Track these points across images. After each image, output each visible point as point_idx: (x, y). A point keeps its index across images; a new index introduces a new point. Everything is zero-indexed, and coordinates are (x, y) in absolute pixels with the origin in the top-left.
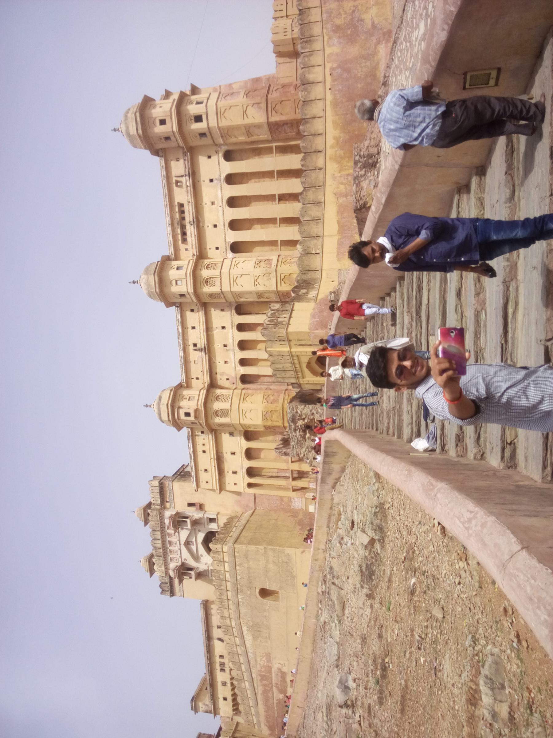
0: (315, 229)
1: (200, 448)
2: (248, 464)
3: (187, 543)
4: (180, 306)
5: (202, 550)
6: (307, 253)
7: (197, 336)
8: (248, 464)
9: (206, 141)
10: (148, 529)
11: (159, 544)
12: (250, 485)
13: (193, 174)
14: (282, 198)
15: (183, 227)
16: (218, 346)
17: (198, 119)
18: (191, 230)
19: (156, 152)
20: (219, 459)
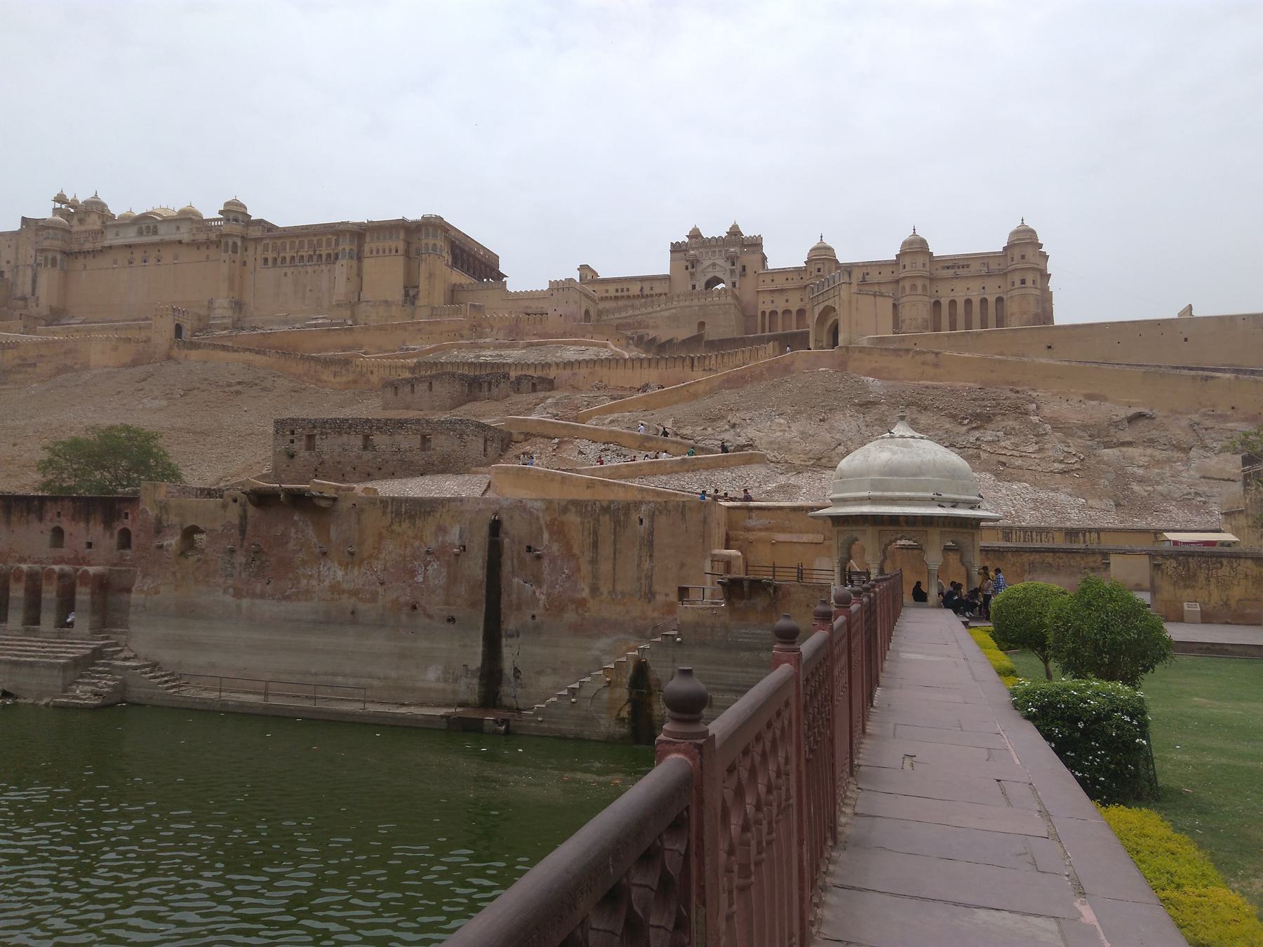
2: (780, 311)
3: (714, 265)
5: (709, 276)
8: (780, 311)
9: (1009, 284)
12: (763, 313)
13: (989, 275)
15: (953, 267)
17: (1023, 282)
18: (951, 272)
20: (782, 290)
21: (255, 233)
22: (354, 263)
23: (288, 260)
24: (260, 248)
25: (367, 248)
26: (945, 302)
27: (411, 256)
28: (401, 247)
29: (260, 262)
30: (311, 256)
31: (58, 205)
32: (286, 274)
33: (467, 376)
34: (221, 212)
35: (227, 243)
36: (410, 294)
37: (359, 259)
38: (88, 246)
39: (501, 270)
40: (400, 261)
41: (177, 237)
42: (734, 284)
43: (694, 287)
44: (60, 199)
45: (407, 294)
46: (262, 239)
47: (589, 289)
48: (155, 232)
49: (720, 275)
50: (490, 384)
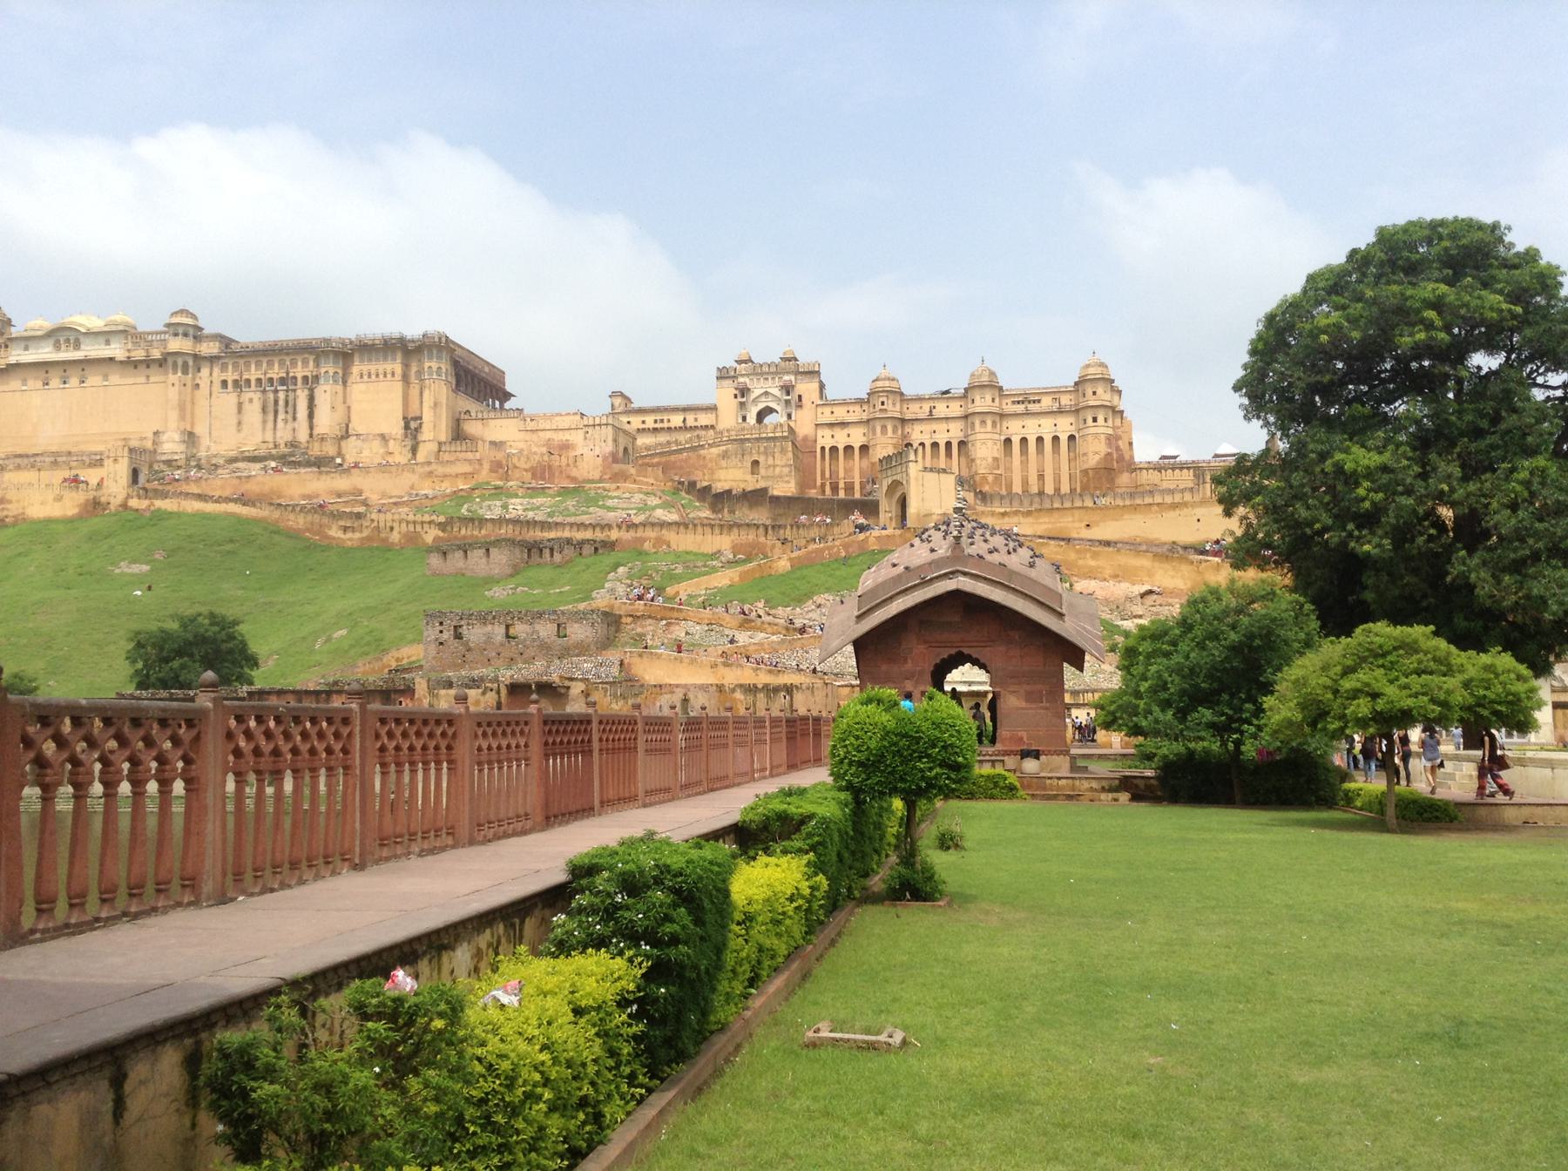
0: (1016, 503)
1: (851, 408)
2: (841, 447)
3: (766, 393)
4: (965, 396)
5: (761, 406)
6: (1002, 497)
7: (941, 409)
8: (841, 447)
10: (777, 360)
11: (765, 369)
13: (1061, 412)
14: (1041, 477)
16: (935, 426)
17: (1095, 420)
18: (1020, 408)
19: (1076, 384)
20: (843, 424)
22: (339, 388)
25: (355, 370)
26: (1016, 440)
30: (283, 381)
32: (251, 401)
36: (412, 427)
39: (508, 388)
40: (399, 386)
42: (789, 416)
43: (744, 419)
45: (407, 427)
47: (624, 419)
49: (773, 405)
50: (552, 550)
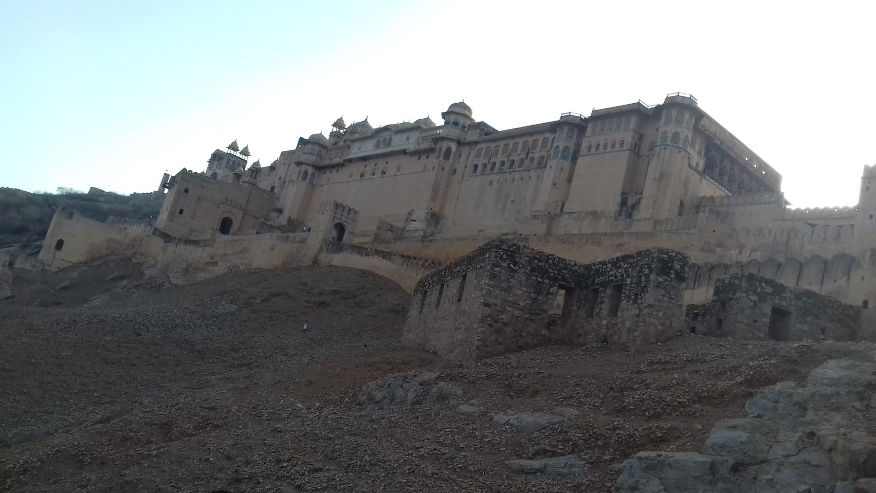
21: (472, 136)
22: (567, 164)
23: (498, 166)
24: (473, 153)
25: (585, 144)
27: (638, 152)
28: (629, 137)
29: (470, 168)
31: (335, 129)
32: (491, 183)
33: (561, 264)
34: (444, 115)
35: (441, 148)
37: (574, 160)
38: (337, 160)
41: (404, 147)
44: (339, 124)
45: (624, 203)
46: (476, 143)
48: (389, 144)
